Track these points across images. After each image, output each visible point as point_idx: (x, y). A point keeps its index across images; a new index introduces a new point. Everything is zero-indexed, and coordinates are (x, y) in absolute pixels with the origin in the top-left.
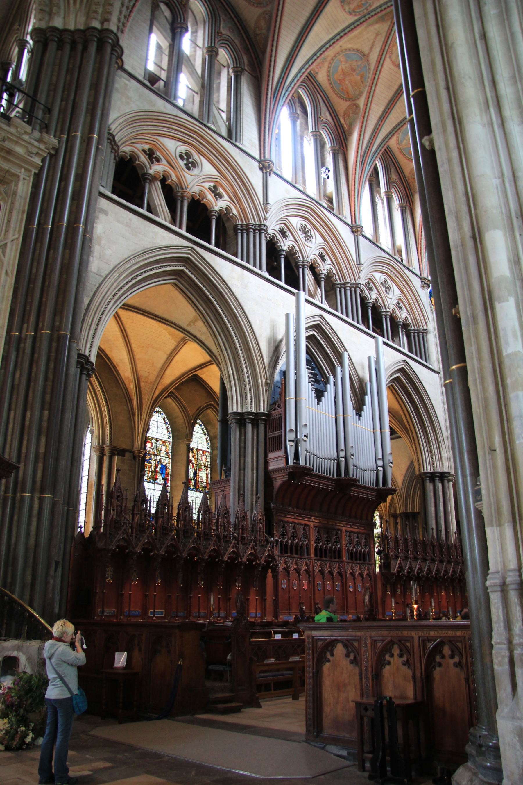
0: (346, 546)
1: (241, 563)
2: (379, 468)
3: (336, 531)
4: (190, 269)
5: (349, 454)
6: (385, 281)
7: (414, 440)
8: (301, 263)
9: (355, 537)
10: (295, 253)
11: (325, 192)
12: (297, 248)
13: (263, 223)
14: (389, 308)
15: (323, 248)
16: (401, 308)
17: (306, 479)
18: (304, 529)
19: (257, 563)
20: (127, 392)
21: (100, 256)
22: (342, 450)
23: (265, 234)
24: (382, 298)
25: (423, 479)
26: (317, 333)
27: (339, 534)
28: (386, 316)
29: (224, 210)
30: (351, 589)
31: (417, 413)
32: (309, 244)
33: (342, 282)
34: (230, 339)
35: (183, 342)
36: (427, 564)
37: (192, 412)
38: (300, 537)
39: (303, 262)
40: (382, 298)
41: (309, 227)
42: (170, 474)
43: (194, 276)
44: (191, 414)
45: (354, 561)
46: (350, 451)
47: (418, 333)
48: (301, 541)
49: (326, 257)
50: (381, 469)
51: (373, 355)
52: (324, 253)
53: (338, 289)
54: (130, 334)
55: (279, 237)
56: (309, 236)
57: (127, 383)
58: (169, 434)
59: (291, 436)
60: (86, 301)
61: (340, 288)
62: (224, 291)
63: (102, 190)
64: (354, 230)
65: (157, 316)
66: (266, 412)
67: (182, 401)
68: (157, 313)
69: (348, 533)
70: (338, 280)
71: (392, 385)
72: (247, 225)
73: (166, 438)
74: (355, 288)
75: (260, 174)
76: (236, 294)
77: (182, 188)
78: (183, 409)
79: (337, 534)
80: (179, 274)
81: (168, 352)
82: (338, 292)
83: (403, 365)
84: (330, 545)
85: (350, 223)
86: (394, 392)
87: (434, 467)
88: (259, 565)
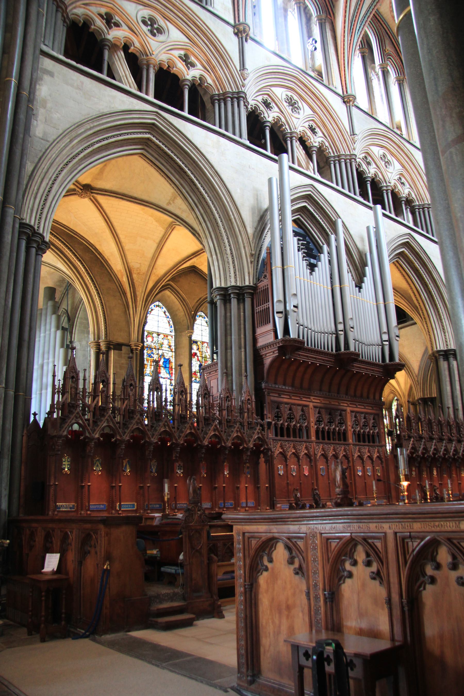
0: (352, 428)
1: (225, 448)
2: (384, 343)
3: (339, 412)
4: (161, 140)
5: (348, 327)
6: (384, 156)
7: (425, 319)
8: (289, 135)
9: (362, 418)
10: (282, 126)
11: (313, 65)
12: (283, 120)
13: (240, 90)
14: (390, 183)
15: (313, 120)
16: (403, 183)
17: (299, 355)
18: (302, 410)
19: (244, 447)
20: (121, 285)
21: (46, 119)
22: (340, 323)
23: (244, 103)
24: (381, 173)
25: (436, 357)
26: (308, 205)
27: (344, 415)
28: (387, 190)
29: (198, 79)
30: (360, 474)
31: (426, 289)
32: (296, 115)
33: (336, 154)
34: (209, 211)
35: (171, 227)
36: (444, 444)
37: (192, 303)
38: (298, 418)
39: (291, 133)
40: (381, 173)
41: (295, 98)
42: (173, 367)
43: (163, 144)
44: (191, 306)
45: (362, 443)
46: (350, 323)
47: (423, 209)
48: (299, 423)
49: (317, 130)
50: (387, 343)
51: (372, 224)
52: (314, 126)
53: (332, 162)
54: (115, 224)
55: (262, 108)
56: (296, 107)
57: (120, 277)
58: (171, 327)
59: (279, 307)
60: (29, 167)
61: (334, 161)
62: (198, 158)
63: (45, 48)
64: (346, 100)
65: (136, 198)
66: (252, 284)
67: (181, 292)
68: (135, 195)
69: (354, 414)
70: (331, 153)
71: (397, 261)
72: (224, 94)
73: (168, 332)
74: (350, 160)
75: (235, 40)
76: (211, 162)
77: (147, 55)
78: (182, 300)
79: (341, 415)
80: (146, 143)
81: (158, 241)
82: (332, 166)
83: (408, 238)
84: (334, 427)
85: (341, 93)
86: (401, 269)
87: (447, 345)
88: (247, 449)
